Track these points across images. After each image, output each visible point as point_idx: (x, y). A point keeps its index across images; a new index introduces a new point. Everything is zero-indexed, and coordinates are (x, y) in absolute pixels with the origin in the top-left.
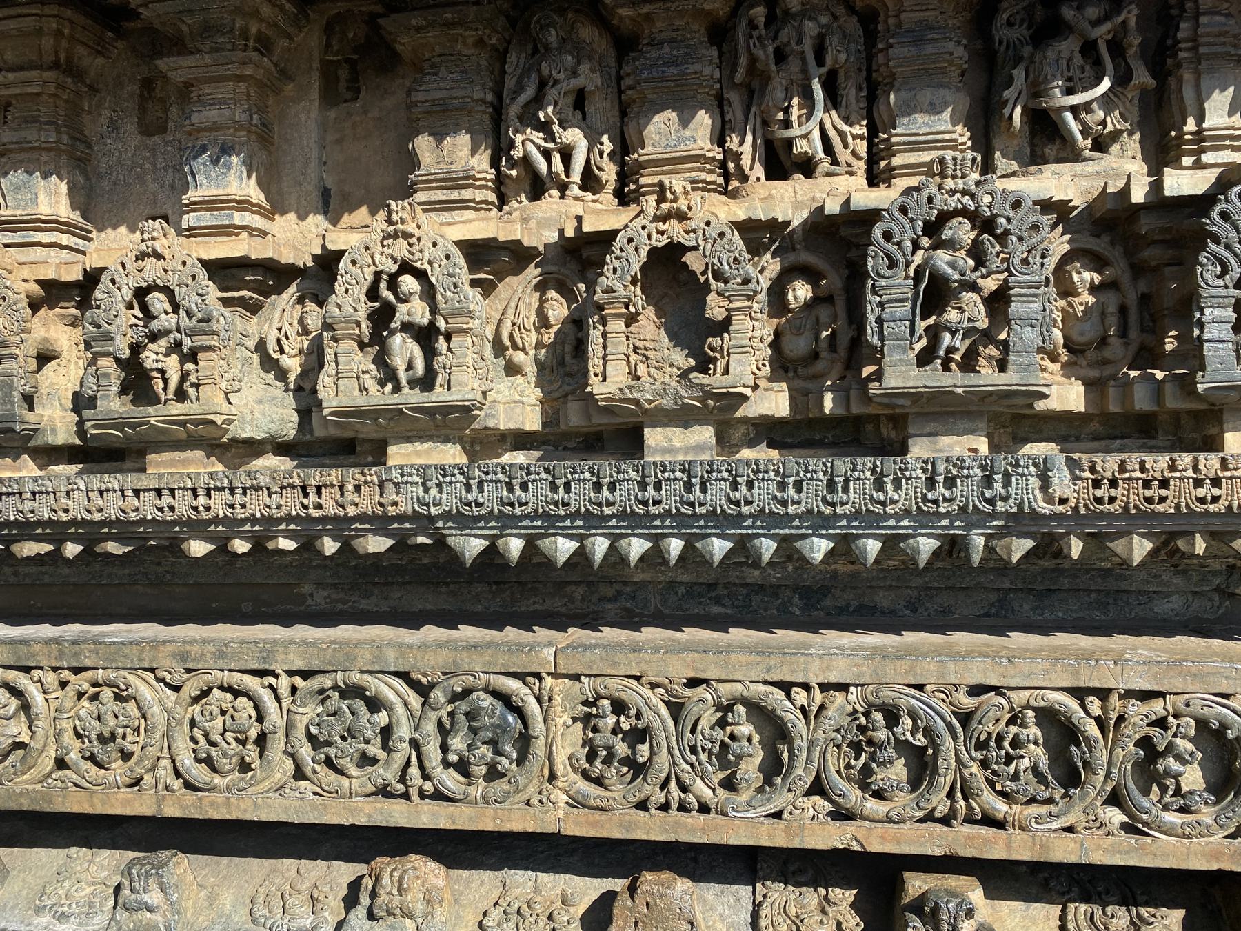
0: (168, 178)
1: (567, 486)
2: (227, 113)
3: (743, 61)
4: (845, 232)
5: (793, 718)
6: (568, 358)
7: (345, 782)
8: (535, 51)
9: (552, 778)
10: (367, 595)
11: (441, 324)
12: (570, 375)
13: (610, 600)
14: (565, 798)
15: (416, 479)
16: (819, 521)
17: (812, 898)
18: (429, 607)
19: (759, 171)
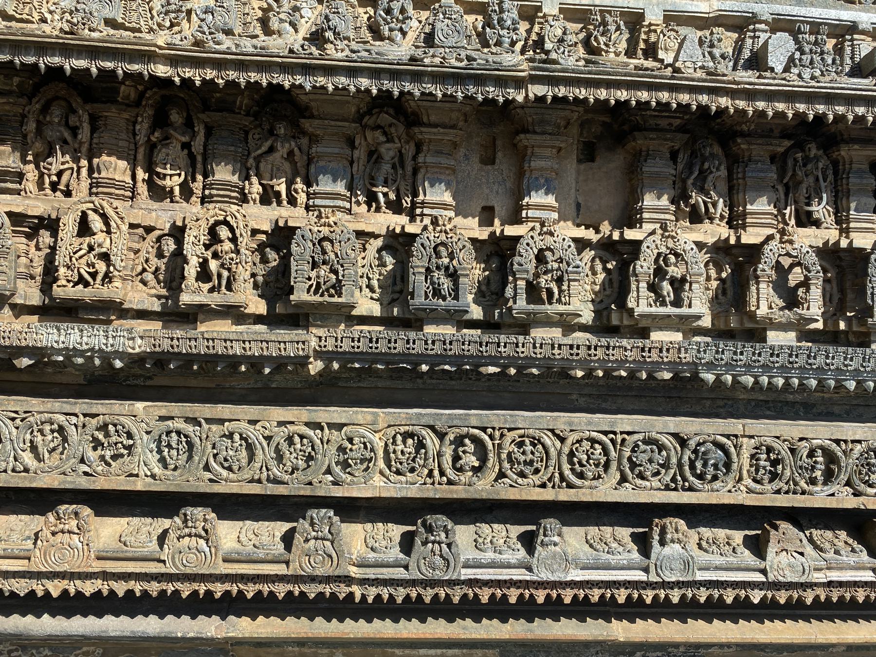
0: (495, 187)
1: (760, 355)
2: (549, 163)
3: (790, 174)
4: (842, 254)
5: (840, 454)
6: (720, 296)
7: (648, 484)
8: (693, 155)
9: (740, 479)
10: (605, 401)
11: (688, 278)
12: (719, 304)
13: (721, 407)
14: (746, 489)
15: (694, 347)
16: (855, 373)
17: (829, 534)
18: (636, 408)
19: (793, 222)
